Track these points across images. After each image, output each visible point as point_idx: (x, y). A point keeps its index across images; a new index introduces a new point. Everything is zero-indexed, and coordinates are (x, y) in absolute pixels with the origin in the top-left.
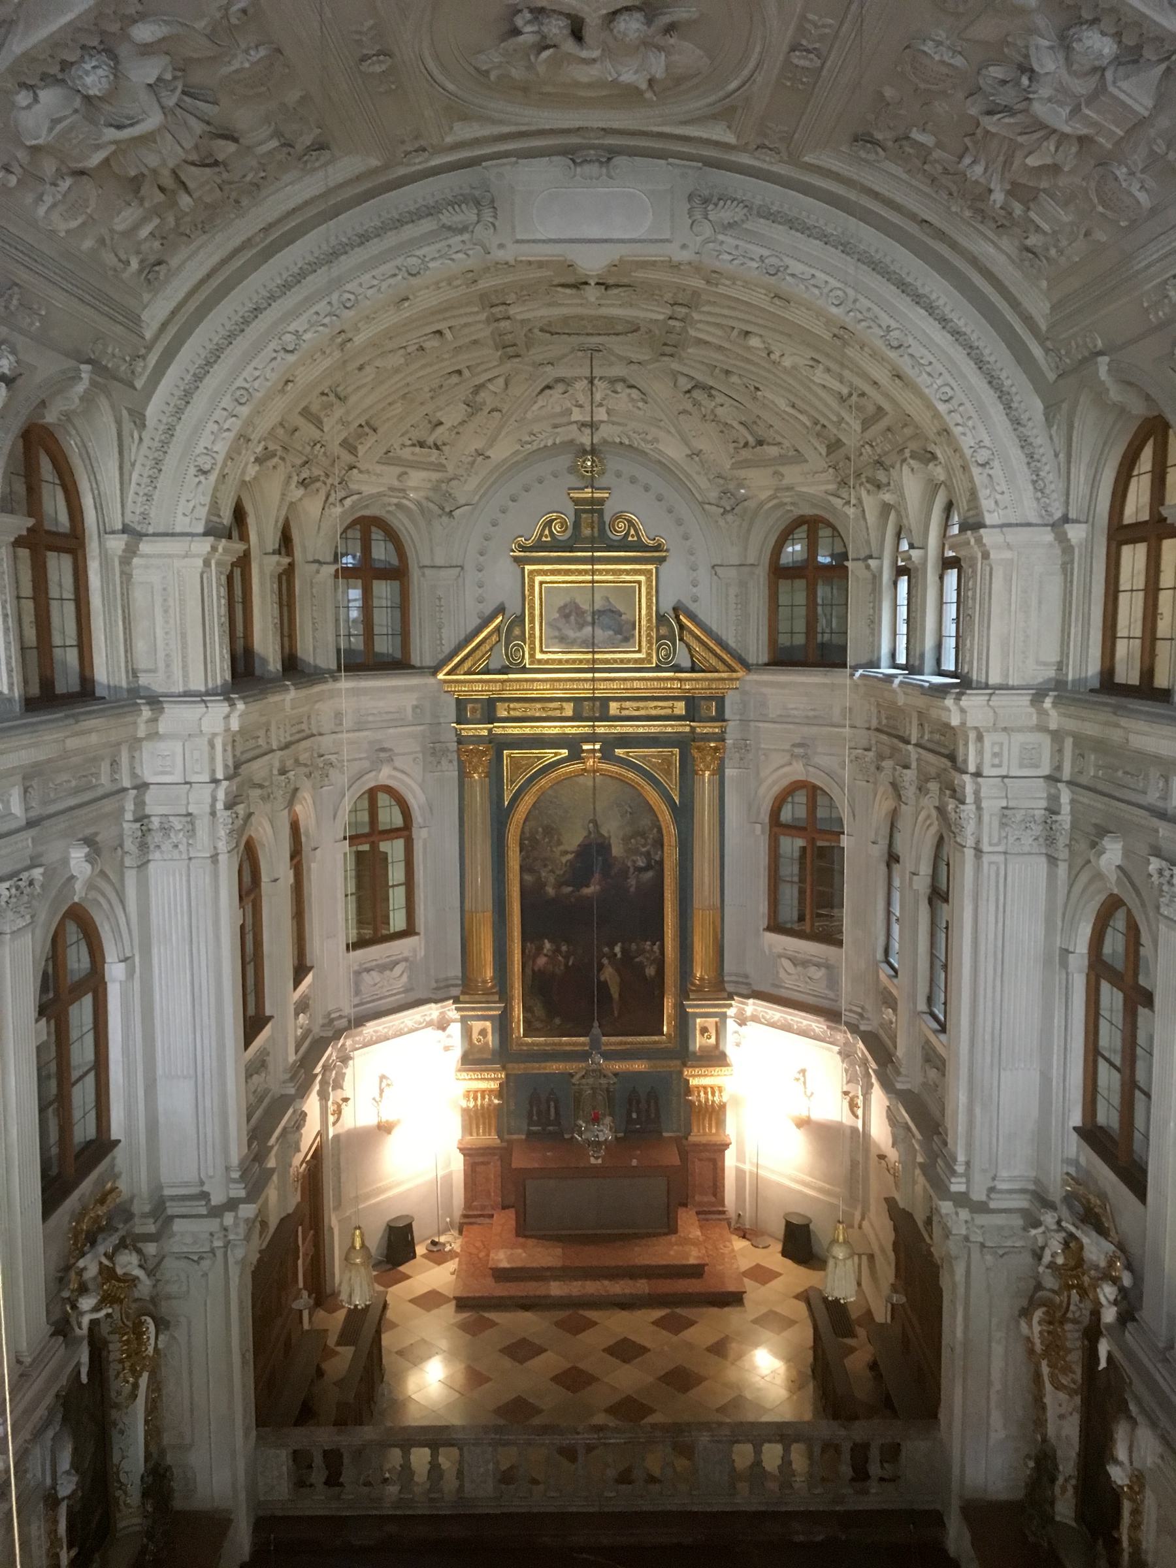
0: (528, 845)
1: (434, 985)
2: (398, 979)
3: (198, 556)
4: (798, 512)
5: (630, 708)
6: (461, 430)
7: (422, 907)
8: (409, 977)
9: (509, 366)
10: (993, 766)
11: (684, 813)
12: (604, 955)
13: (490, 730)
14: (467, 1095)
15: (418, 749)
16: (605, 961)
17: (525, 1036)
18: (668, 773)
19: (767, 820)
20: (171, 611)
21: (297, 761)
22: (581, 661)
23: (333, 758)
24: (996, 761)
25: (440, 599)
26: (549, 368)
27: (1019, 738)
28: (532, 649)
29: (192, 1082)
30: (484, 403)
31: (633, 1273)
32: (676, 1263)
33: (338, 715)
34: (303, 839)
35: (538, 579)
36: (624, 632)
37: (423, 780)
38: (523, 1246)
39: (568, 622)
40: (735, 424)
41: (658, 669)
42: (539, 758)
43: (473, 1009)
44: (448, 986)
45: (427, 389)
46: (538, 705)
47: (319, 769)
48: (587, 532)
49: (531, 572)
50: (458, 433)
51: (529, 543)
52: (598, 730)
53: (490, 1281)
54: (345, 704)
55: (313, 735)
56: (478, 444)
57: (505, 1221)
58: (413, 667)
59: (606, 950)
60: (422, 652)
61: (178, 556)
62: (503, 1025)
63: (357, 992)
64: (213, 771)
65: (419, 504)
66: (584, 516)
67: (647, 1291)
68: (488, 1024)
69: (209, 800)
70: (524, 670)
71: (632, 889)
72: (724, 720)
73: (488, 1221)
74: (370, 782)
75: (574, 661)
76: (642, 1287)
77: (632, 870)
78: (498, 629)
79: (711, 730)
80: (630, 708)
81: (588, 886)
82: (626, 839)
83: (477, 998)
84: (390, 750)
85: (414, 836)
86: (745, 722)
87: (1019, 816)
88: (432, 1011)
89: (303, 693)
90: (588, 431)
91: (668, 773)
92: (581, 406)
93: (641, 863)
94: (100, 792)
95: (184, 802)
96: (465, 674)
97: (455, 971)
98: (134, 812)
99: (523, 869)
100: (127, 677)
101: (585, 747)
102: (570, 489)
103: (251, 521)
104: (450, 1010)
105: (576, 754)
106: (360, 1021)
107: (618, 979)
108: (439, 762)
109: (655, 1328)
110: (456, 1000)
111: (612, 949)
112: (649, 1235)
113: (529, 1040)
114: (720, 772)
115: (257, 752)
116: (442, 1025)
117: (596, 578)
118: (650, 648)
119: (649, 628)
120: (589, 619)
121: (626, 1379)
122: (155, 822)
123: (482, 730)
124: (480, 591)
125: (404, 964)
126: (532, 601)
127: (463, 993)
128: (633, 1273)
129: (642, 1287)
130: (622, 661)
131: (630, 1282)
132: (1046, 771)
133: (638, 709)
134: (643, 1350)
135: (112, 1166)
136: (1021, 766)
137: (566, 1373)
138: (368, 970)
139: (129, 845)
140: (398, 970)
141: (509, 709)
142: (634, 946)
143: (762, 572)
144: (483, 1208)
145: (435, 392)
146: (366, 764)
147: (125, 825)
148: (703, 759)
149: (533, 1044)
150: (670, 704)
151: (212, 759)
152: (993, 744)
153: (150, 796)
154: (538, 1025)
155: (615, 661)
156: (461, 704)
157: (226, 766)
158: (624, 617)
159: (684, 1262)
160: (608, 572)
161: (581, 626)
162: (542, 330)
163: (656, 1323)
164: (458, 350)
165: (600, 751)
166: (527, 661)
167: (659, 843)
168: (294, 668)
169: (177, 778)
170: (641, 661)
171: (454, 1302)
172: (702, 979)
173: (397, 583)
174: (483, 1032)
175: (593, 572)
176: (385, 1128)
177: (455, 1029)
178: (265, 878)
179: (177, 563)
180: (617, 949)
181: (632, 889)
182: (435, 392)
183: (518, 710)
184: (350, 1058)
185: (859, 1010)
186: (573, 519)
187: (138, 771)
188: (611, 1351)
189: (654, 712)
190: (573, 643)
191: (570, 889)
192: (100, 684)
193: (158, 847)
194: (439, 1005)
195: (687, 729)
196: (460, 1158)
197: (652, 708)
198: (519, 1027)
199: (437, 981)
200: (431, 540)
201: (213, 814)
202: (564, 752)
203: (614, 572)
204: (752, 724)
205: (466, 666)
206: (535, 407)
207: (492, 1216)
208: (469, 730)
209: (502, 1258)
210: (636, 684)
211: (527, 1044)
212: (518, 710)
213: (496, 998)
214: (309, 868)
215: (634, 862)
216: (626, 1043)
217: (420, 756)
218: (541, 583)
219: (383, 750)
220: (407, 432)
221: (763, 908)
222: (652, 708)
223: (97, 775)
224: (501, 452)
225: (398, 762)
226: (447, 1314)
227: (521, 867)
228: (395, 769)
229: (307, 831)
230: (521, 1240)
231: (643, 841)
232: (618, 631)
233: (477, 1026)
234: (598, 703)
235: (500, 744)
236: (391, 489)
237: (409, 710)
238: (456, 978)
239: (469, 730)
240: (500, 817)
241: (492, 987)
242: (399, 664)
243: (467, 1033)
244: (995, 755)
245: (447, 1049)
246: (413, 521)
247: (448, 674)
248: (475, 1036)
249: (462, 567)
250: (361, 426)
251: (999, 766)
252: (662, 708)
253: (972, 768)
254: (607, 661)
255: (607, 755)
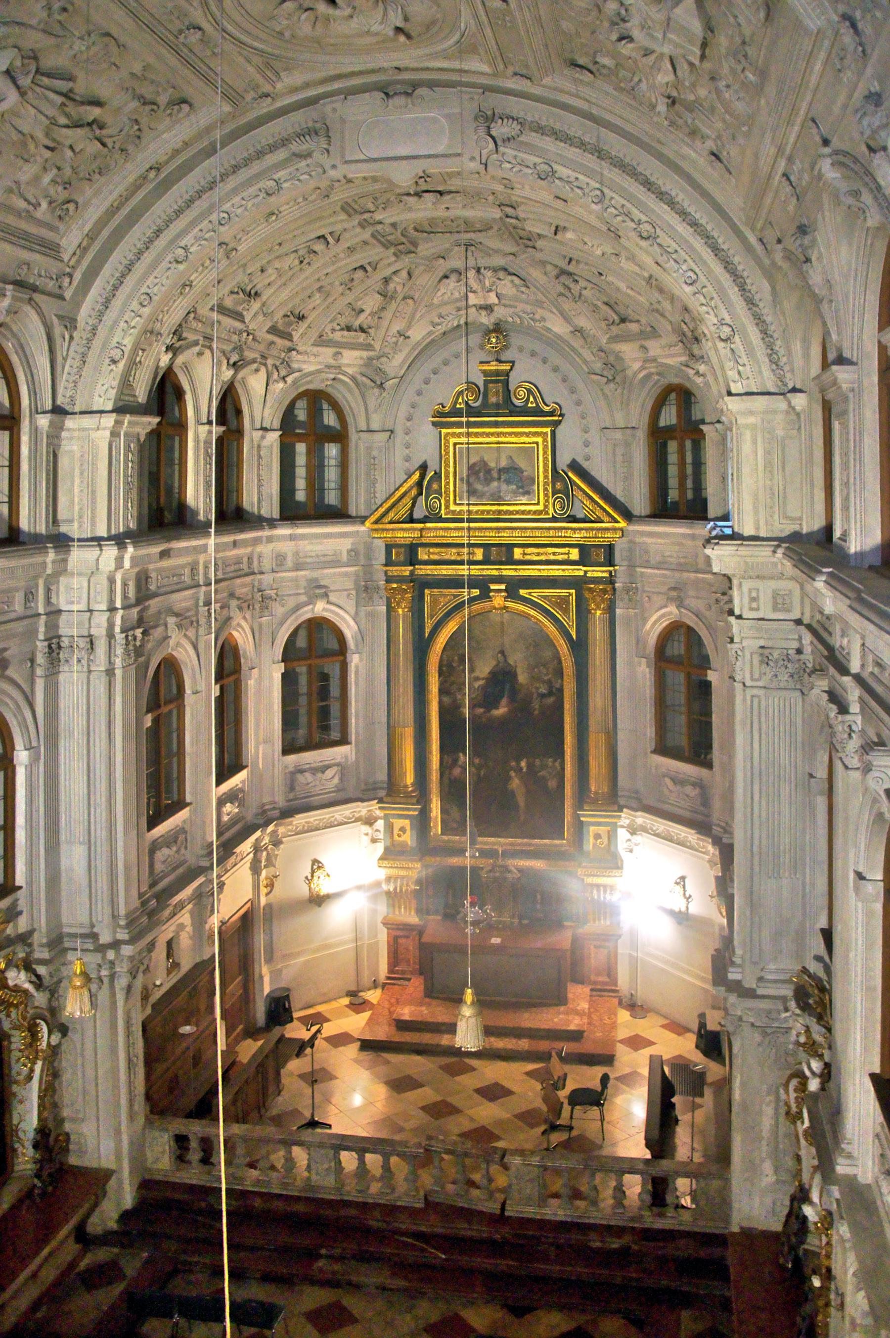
0: (447, 670)
1: (363, 786)
2: (331, 780)
3: (104, 429)
4: (665, 382)
5: (532, 554)
6: (382, 315)
7: (353, 720)
8: (341, 779)
9: (406, 260)
10: (751, 609)
11: (579, 647)
12: (512, 769)
13: (412, 572)
14: (388, 879)
15: (352, 587)
16: (513, 774)
17: (442, 834)
18: (566, 611)
19: (652, 656)
20: (86, 474)
21: (232, 595)
22: (488, 512)
23: (272, 593)
24: (754, 605)
25: (374, 458)
26: (441, 261)
27: (773, 584)
28: (447, 502)
29: (86, 847)
30: (395, 291)
31: (518, 1033)
32: (559, 1027)
33: (280, 559)
34: (242, 661)
35: (452, 440)
36: (525, 485)
37: (357, 613)
38: (429, 1005)
39: (478, 478)
40: (599, 304)
41: (554, 519)
42: (455, 596)
43: (394, 809)
44: (375, 789)
45: (337, 283)
46: (454, 550)
47: (259, 602)
48: (493, 400)
49: (447, 435)
50: (380, 318)
51: (447, 409)
52: (505, 573)
53: (394, 1028)
54: (287, 547)
55: (253, 573)
56: (396, 327)
57: (416, 985)
58: (350, 517)
59: (513, 764)
60: (357, 504)
61: (92, 429)
62: (422, 822)
63: (292, 788)
64: (112, 601)
65: (353, 378)
66: (491, 385)
67: (526, 1048)
68: (407, 822)
69: (105, 624)
70: (441, 520)
71: (536, 712)
72: (613, 566)
73: (406, 983)
74: (306, 613)
75: (483, 512)
76: (524, 1044)
77: (535, 696)
78: (419, 484)
79: (600, 575)
80: (532, 554)
81: (497, 708)
82: (531, 668)
83: (398, 800)
84: (325, 587)
85: (348, 660)
86: (632, 567)
87: (776, 654)
88: (362, 809)
89: (228, 539)
90: (484, 313)
91: (566, 611)
92: (474, 292)
93: (543, 690)
94: (12, 616)
95: (87, 626)
96: (390, 523)
97: (382, 775)
98: (46, 633)
99: (442, 692)
100: (47, 526)
101: (493, 587)
102: (481, 363)
103: (189, 397)
104: (372, 807)
105: (485, 594)
106: (287, 813)
107: (523, 790)
108: (371, 598)
109: (525, 1077)
110: (381, 801)
111: (518, 761)
112: (534, 1006)
113: (445, 838)
114: (611, 610)
115: (176, 587)
116: (369, 821)
117: (471, 440)
118: (547, 501)
119: (546, 484)
120: (495, 475)
121: (487, 1113)
122: (65, 642)
123: (406, 571)
124: (407, 451)
125: (335, 769)
126: (447, 460)
127: (388, 795)
128: (518, 1033)
129: (524, 1044)
130: (523, 512)
131: (514, 1041)
132: (796, 615)
133: (538, 554)
134: (508, 1093)
135: (15, 903)
136: (775, 609)
137: (435, 1104)
138: (302, 771)
139: (40, 659)
140: (329, 773)
141: (429, 553)
142: (538, 762)
143: (642, 435)
144: (403, 972)
145: (349, 285)
146: (303, 598)
147: (38, 643)
148: (594, 599)
149: (449, 841)
150: (566, 550)
151: (112, 591)
152: (750, 591)
153: (63, 619)
154: (455, 825)
155: (517, 512)
156: (389, 548)
157: (125, 597)
158: (525, 474)
159: (564, 1028)
160: (510, 434)
161: (488, 480)
162: (416, 230)
163: (529, 1074)
164: (351, 250)
165: (506, 590)
166: (443, 512)
167: (560, 673)
168: (232, 515)
169: (83, 606)
170: (540, 512)
171: (359, 1043)
172: (596, 793)
173: (339, 445)
174: (403, 829)
175: (468, 435)
176: (318, 901)
177: (380, 824)
178: (188, 691)
179: (93, 435)
180: (523, 764)
181: (536, 712)
182: (349, 285)
183: (436, 554)
184: (281, 842)
185: (723, 824)
186: (482, 390)
187: (54, 600)
188: (478, 1091)
189: (552, 557)
190: (481, 496)
191: (482, 710)
192: (24, 532)
193: (67, 661)
194: (365, 804)
195: (581, 573)
196: (385, 930)
197: (550, 553)
198: (436, 827)
199: (366, 784)
200: (366, 409)
201: (111, 636)
202: (476, 592)
203: (516, 434)
204: (638, 569)
205: (391, 515)
206: (439, 294)
207: (409, 980)
208: (394, 571)
209: (406, 1013)
210: (538, 533)
211: (444, 841)
212: (436, 554)
213: (415, 800)
214: (247, 684)
215: (537, 688)
216: (530, 845)
217: (354, 592)
218: (455, 444)
219: (319, 587)
220: (335, 319)
221: (650, 732)
222: (550, 553)
223: (10, 603)
224: (418, 334)
225: (333, 597)
226: (352, 1050)
227: (440, 690)
228: (328, 602)
229: (245, 652)
230: (427, 1000)
231: (544, 671)
232: (522, 487)
233: (398, 823)
234: (504, 549)
235: (421, 585)
236: (328, 367)
237: (345, 554)
238: (382, 782)
239: (394, 571)
240: (421, 647)
241: (412, 791)
242: (339, 514)
243: (389, 828)
244: (754, 599)
245: (374, 841)
246: (352, 394)
247: (376, 522)
248: (396, 832)
249: (392, 431)
250: (286, 316)
251: (757, 609)
252: (560, 554)
253: (737, 612)
254: (511, 513)
255: (512, 592)
